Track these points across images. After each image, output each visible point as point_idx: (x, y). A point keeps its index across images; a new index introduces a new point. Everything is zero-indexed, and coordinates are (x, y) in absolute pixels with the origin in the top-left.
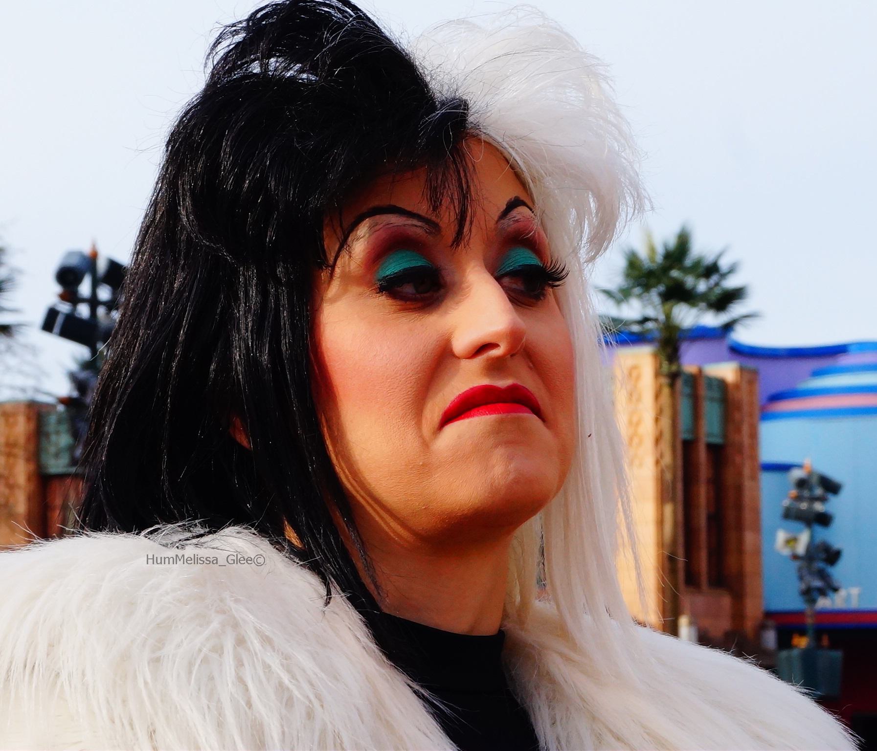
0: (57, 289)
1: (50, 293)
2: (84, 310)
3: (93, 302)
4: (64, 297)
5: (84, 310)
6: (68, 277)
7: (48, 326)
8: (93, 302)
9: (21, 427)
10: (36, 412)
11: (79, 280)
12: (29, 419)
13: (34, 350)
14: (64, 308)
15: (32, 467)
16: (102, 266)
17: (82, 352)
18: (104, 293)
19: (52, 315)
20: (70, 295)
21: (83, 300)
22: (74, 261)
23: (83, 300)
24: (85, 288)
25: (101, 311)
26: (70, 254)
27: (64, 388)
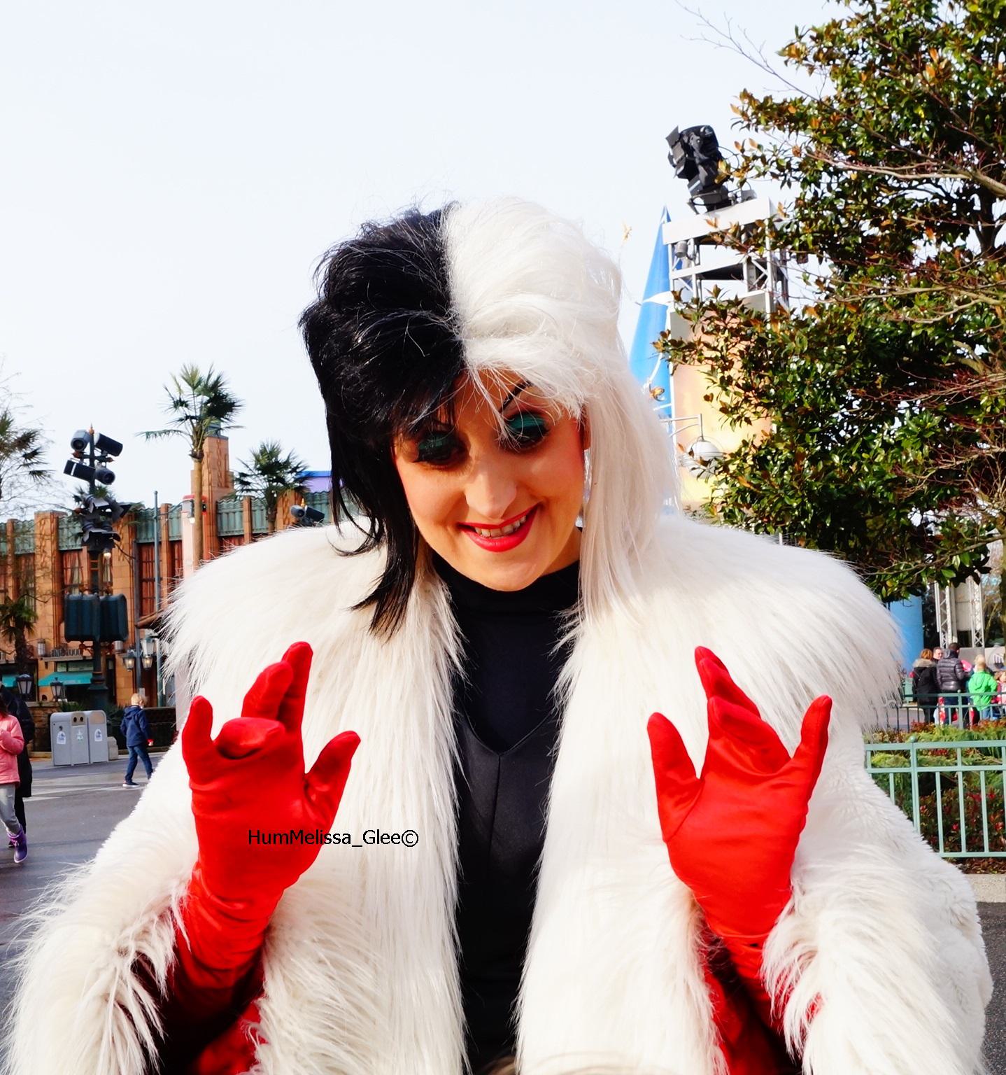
0: (73, 451)
1: (69, 453)
2: (87, 462)
3: (92, 458)
4: (75, 455)
5: (87, 462)
6: (78, 444)
7: (67, 471)
8: (92, 458)
9: (48, 526)
10: (56, 518)
11: (84, 446)
12: (52, 522)
13: (62, 484)
14: (77, 461)
15: (54, 546)
16: (96, 439)
17: (84, 485)
18: (98, 453)
19: (70, 464)
20: (79, 454)
21: (86, 457)
22: (81, 436)
23: (86, 457)
24: (87, 451)
25: (96, 462)
26: (78, 432)
27: (74, 506)
